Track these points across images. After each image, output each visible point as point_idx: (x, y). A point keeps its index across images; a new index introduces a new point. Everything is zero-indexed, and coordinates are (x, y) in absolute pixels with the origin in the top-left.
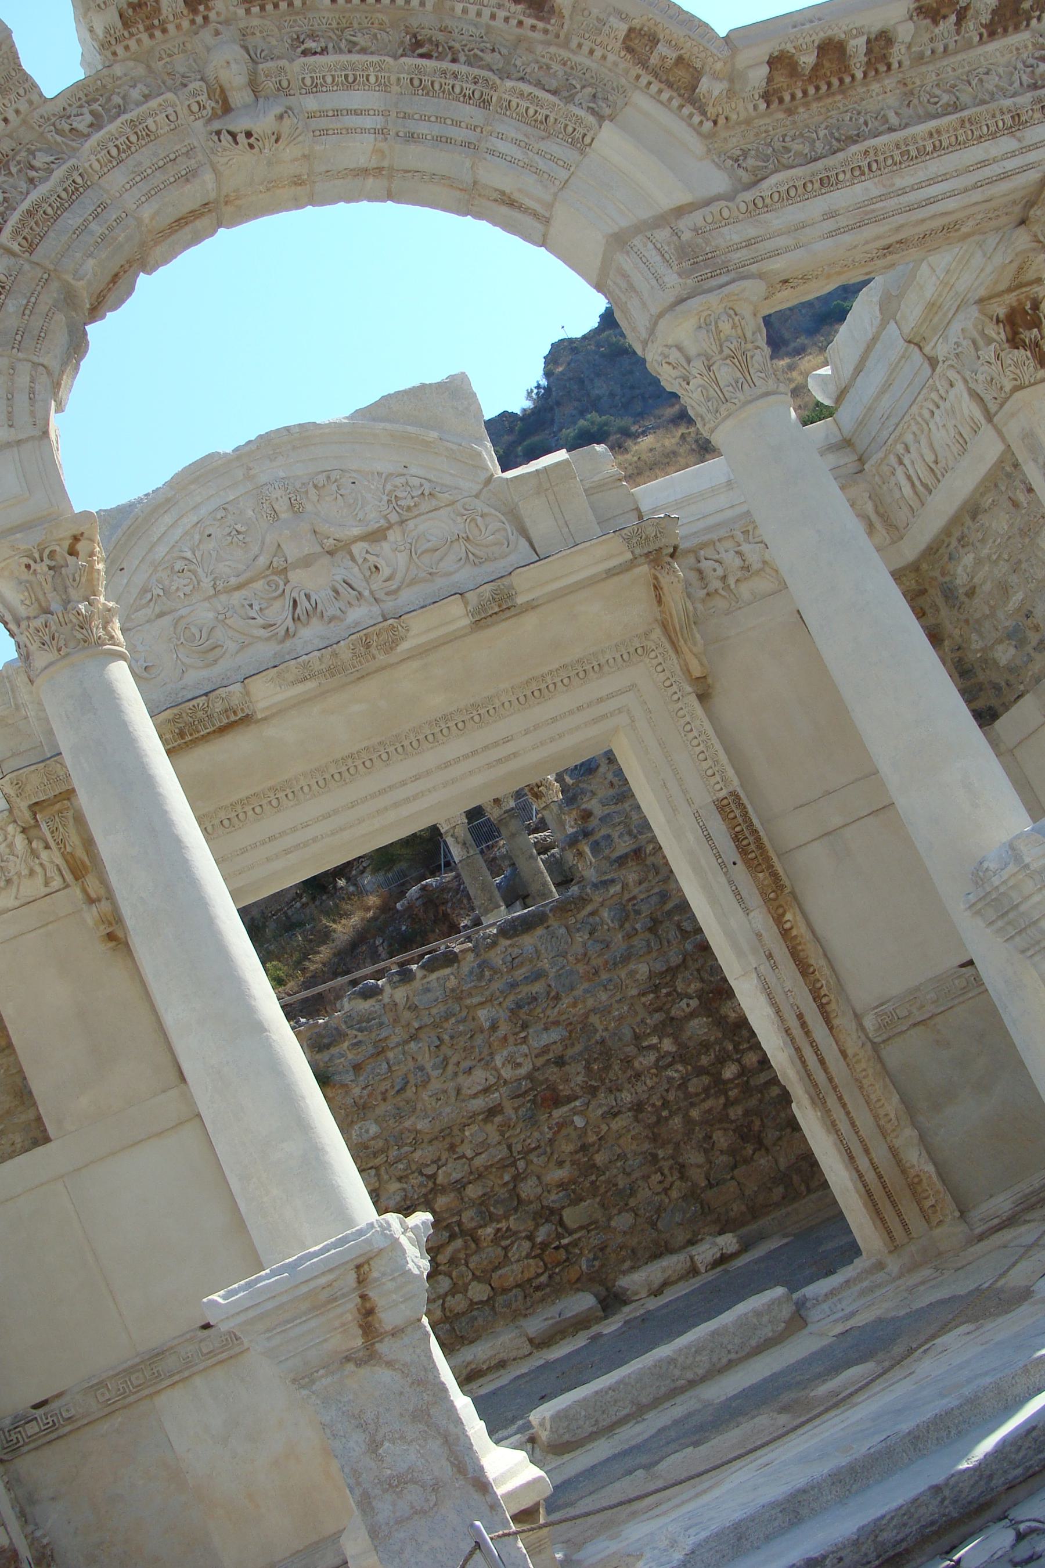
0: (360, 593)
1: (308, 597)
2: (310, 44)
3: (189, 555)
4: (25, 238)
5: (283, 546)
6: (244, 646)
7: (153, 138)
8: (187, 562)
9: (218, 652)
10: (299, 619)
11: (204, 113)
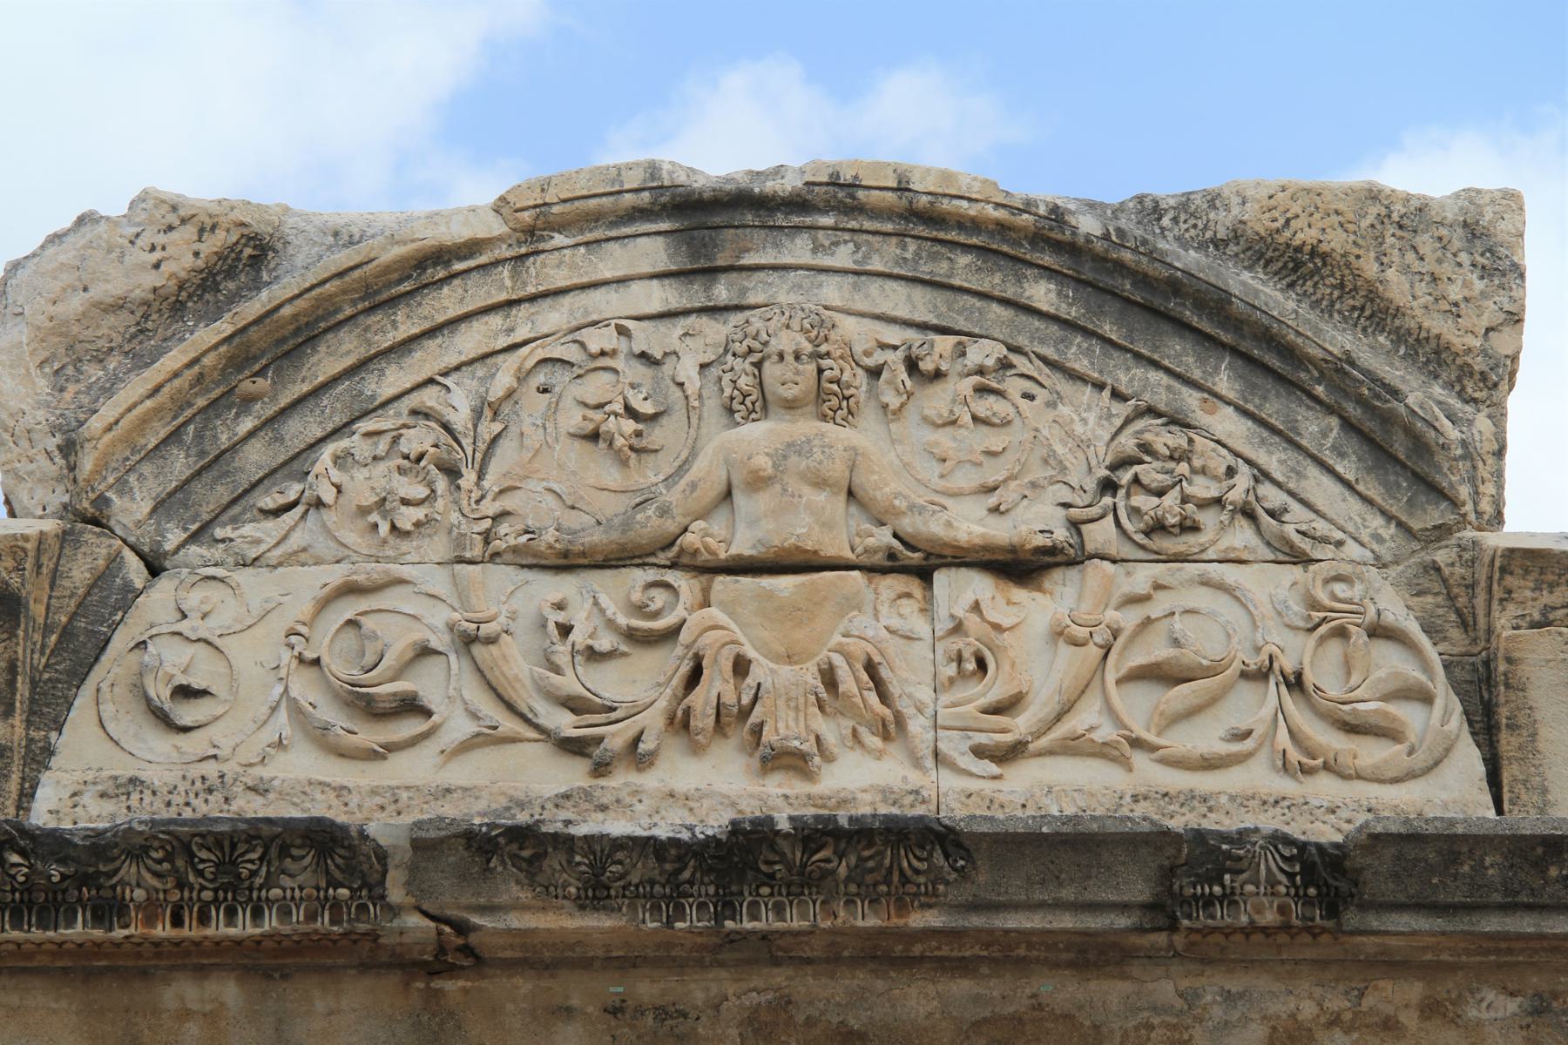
0: (900, 721)
1: (741, 667)
3: (460, 418)
5: (739, 498)
6: (488, 739)
8: (445, 438)
9: (409, 727)
10: (686, 725)
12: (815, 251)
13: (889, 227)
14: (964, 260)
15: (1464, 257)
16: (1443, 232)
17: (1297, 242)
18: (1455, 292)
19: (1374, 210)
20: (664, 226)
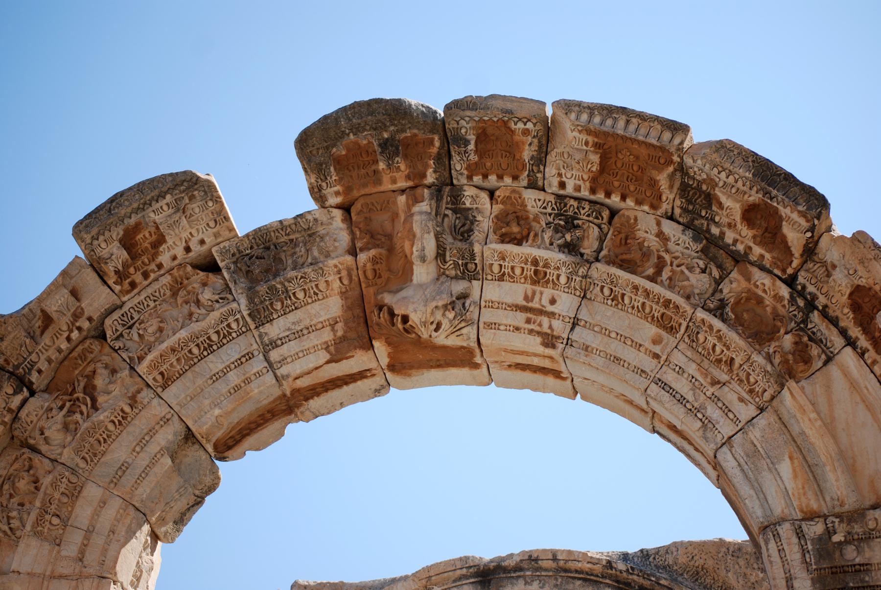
2: (515, 229)
4: (162, 374)
7: (320, 297)
11: (379, 281)
12: (525, 584)
13: (551, 574)
14: (578, 583)
15: (755, 566)
16: (748, 556)
17: (697, 564)
18: (753, 579)
19: (724, 550)
20: (472, 580)
